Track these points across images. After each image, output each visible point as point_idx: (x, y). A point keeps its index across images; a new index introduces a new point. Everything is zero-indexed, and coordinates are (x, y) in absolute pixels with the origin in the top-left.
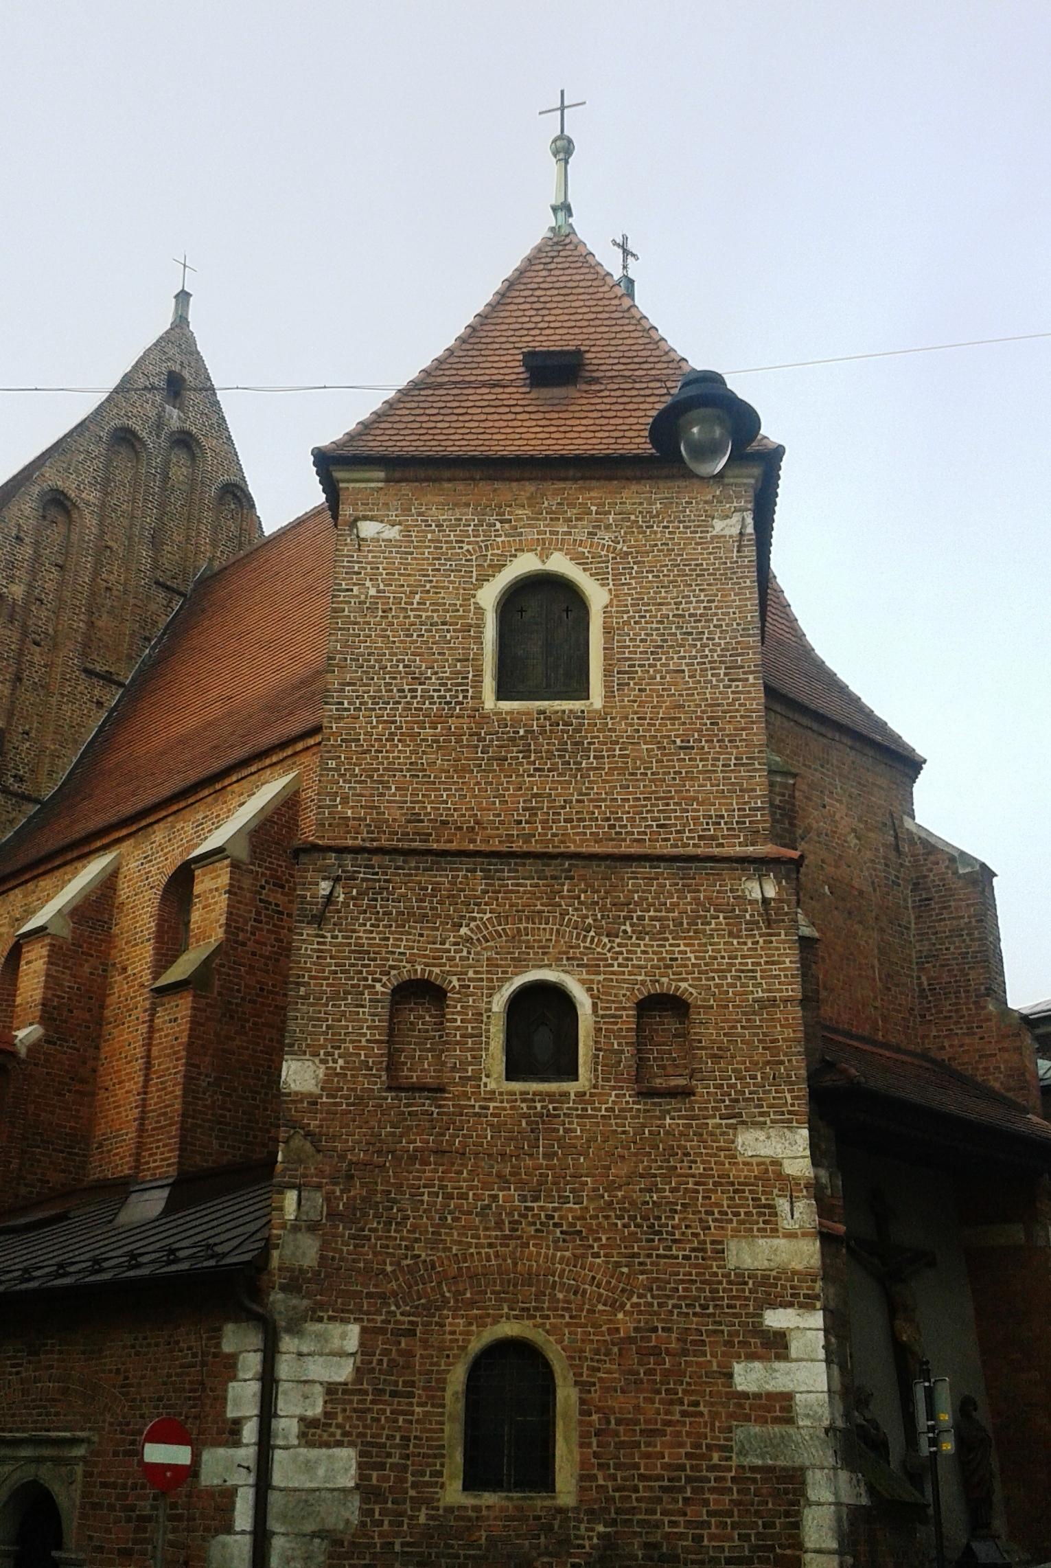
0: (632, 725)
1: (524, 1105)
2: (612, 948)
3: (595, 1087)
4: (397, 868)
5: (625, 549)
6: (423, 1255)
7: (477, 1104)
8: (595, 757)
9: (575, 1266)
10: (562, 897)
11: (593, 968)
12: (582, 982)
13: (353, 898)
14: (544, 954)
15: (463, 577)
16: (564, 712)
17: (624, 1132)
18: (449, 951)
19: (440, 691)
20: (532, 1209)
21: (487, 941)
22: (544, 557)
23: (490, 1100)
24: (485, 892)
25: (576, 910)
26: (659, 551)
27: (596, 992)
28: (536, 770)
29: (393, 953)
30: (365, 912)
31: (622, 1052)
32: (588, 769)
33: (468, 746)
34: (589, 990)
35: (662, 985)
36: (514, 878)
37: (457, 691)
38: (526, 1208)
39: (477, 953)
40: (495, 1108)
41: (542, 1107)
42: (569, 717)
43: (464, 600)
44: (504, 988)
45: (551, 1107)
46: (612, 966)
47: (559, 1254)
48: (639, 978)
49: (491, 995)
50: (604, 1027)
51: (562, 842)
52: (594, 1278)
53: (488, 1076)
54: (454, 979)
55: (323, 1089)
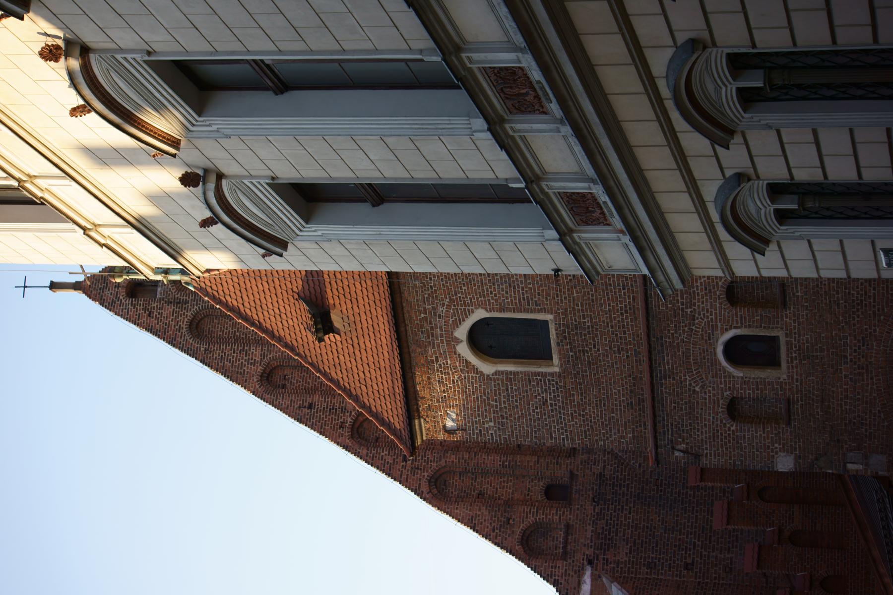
1: (795, 362)
2: (701, 318)
3: (782, 328)
4: (664, 420)
6: (878, 409)
7: (796, 383)
8: (584, 318)
9: (881, 340)
10: (673, 342)
11: (714, 328)
12: (722, 333)
13: (683, 440)
14: (707, 351)
16: (557, 334)
17: (807, 315)
18: (710, 396)
20: (851, 359)
21: (702, 378)
22: (458, 341)
23: (793, 378)
24: (674, 379)
25: (680, 335)
26: (447, 283)
27: (728, 327)
29: (713, 422)
30: (691, 435)
31: (761, 315)
32: (592, 322)
34: (727, 330)
35: (721, 294)
36: (664, 364)
38: (851, 361)
39: (710, 383)
40: (797, 375)
41: (795, 353)
42: (560, 331)
44: (728, 370)
45: (794, 349)
46: (712, 319)
47: (875, 348)
48: (718, 305)
49: (734, 377)
50: (747, 324)
51: (638, 336)
52: (887, 332)
53: (779, 378)
54: (725, 394)
55: (792, 453)
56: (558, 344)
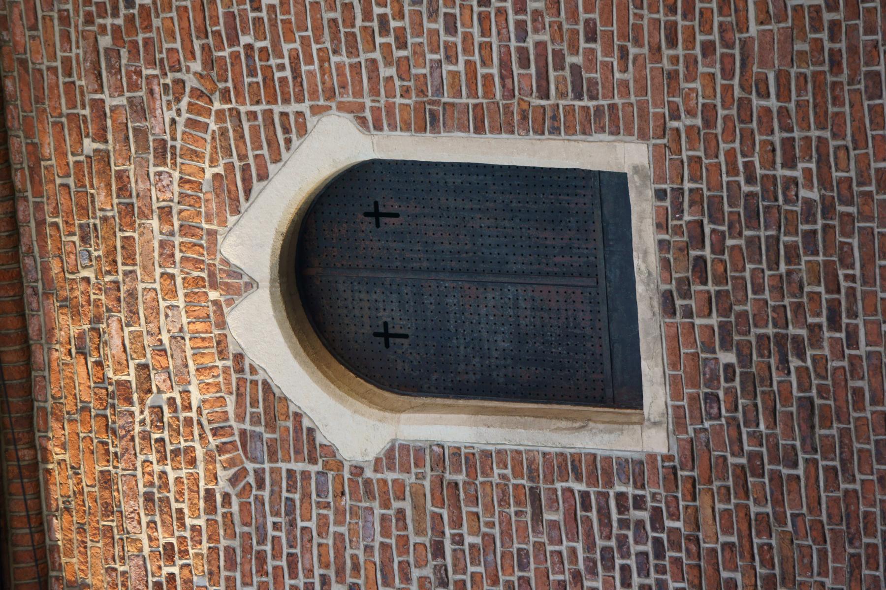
0: (691, 62)
5: (196, 66)
8: (790, 162)
15: (306, 496)
16: (663, 245)
19: (625, 569)
28: (834, 322)
32: (825, 182)
33: (778, 502)
37: (624, 524)
42: (678, 230)
43: (370, 495)
56: (668, 304)
